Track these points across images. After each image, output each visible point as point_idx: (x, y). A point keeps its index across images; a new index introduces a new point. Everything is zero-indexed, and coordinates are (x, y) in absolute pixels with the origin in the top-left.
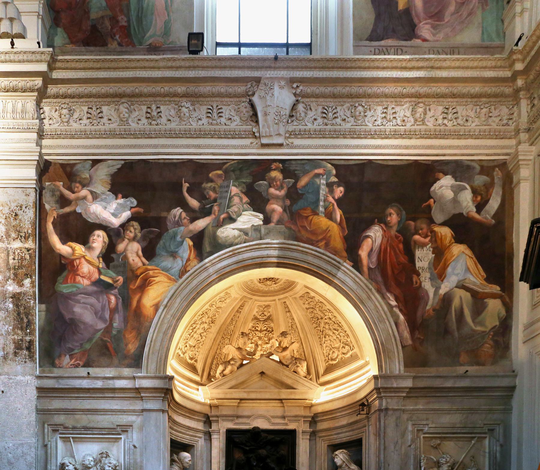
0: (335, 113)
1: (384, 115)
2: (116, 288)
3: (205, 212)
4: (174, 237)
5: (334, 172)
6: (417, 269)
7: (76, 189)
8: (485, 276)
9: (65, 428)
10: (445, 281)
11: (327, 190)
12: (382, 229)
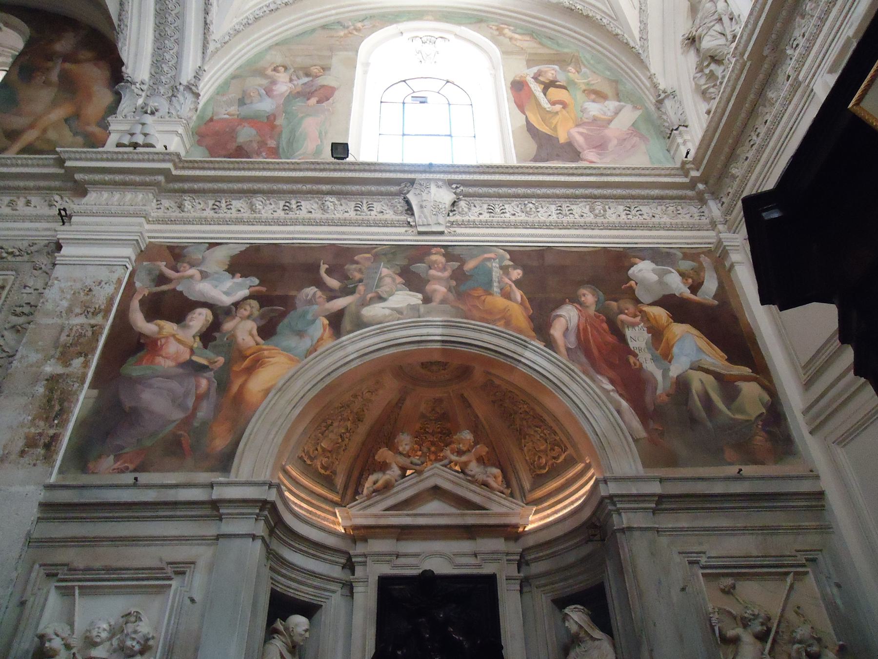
0: (502, 209)
1: (559, 211)
2: (211, 370)
3: (347, 291)
4: (304, 316)
5: (508, 256)
6: (633, 349)
7: (182, 269)
8: (727, 357)
9: (70, 570)
10: (672, 363)
11: (501, 272)
12: (577, 308)
